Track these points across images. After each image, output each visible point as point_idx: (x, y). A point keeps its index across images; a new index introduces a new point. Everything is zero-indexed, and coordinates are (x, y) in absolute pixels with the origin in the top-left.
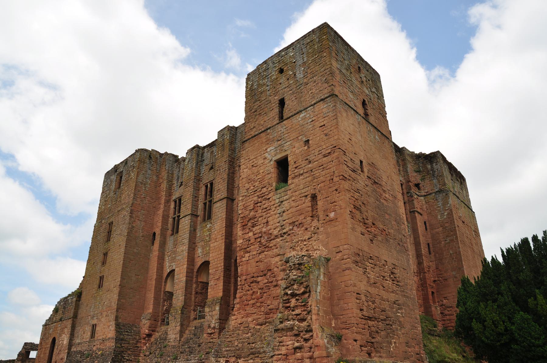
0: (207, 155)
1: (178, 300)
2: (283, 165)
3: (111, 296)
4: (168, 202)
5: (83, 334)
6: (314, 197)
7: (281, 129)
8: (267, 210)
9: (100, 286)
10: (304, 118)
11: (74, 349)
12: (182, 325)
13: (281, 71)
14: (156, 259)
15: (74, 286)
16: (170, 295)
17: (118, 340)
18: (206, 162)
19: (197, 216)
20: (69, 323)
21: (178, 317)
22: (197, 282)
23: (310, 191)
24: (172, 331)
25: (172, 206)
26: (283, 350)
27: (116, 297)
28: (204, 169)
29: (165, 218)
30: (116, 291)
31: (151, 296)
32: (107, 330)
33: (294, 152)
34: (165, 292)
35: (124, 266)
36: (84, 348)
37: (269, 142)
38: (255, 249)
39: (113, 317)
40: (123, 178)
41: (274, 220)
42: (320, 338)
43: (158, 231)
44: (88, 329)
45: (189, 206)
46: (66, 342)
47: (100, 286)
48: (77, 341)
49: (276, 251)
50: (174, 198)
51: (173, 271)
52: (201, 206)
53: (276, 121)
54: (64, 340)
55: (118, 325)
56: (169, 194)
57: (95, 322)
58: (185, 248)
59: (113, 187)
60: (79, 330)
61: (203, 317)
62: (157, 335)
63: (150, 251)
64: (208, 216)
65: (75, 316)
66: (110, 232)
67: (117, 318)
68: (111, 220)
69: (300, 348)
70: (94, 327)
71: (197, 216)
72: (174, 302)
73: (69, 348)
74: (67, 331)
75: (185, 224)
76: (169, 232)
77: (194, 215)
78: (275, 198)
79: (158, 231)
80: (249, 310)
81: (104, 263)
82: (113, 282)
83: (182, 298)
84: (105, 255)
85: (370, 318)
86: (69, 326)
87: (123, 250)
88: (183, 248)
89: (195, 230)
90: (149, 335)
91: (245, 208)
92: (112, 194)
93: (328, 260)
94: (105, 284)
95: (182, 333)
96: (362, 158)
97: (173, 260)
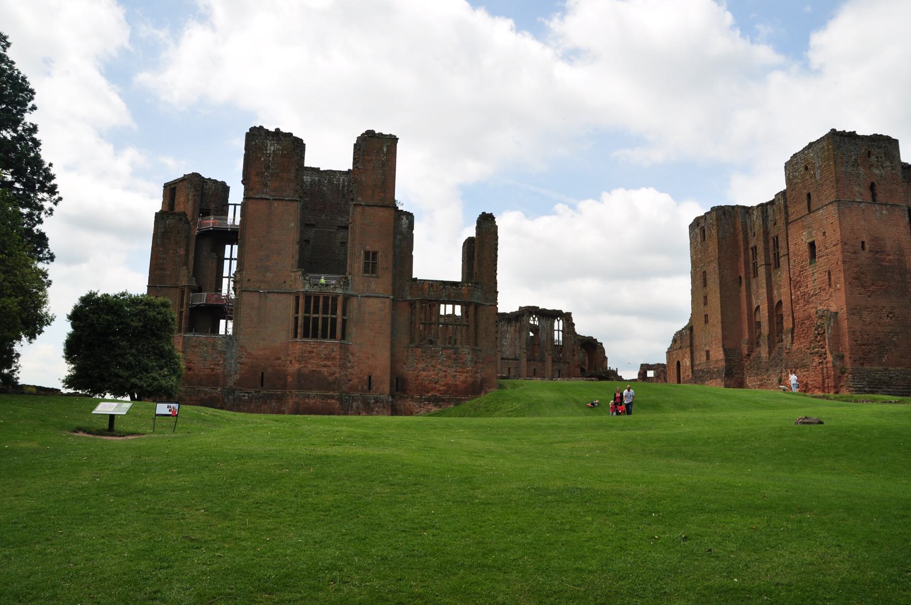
0: (770, 211)
1: (765, 329)
2: (812, 245)
3: (716, 330)
4: (746, 249)
5: (701, 358)
6: (829, 273)
7: (809, 219)
8: (806, 277)
9: (706, 322)
10: (822, 214)
11: (695, 368)
12: (769, 347)
13: (806, 168)
14: (745, 298)
15: (685, 323)
16: (759, 324)
17: (727, 360)
18: (770, 218)
19: (770, 264)
20: (688, 350)
21: (766, 342)
22: (777, 315)
23: (826, 268)
24: (763, 351)
25: (751, 253)
26: (815, 364)
27: (720, 330)
28: (770, 224)
29: (747, 263)
30: (719, 326)
31: (745, 326)
32: (718, 354)
33: (818, 239)
34: (756, 323)
35: (722, 307)
36: (703, 367)
37: (803, 227)
38: (801, 302)
39: (720, 345)
40: (706, 233)
41: (810, 285)
42: (830, 358)
43: (743, 275)
44: (704, 354)
45: (763, 257)
46: (688, 363)
47: (706, 322)
48: (697, 362)
49: (813, 305)
50: (751, 246)
51: (758, 307)
52: (772, 256)
53: (807, 212)
54: (687, 362)
55: (725, 350)
56: (746, 243)
57: (708, 348)
58: (765, 290)
59: (699, 239)
60: (697, 355)
61: (782, 341)
62: (754, 354)
63: (739, 292)
64: (777, 266)
65: (691, 345)
66: (705, 280)
67: (723, 346)
68: (705, 269)
69: (822, 363)
70: (708, 352)
71: (770, 264)
72: (762, 331)
73: (692, 368)
74: (688, 355)
75: (762, 271)
76: (752, 275)
77: (767, 264)
78: (810, 270)
79: (743, 275)
80: (802, 340)
81: (705, 304)
82: (716, 318)
83: (767, 328)
84: (705, 297)
85: (864, 345)
86: (689, 352)
87: (718, 295)
88: (763, 291)
89: (770, 276)
90: (749, 355)
91: (794, 274)
92: (700, 246)
93: (836, 313)
94: (710, 321)
95: (770, 353)
96: (864, 239)
97: (758, 298)
